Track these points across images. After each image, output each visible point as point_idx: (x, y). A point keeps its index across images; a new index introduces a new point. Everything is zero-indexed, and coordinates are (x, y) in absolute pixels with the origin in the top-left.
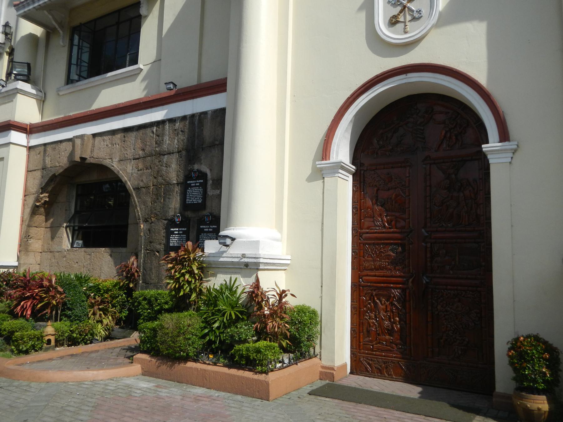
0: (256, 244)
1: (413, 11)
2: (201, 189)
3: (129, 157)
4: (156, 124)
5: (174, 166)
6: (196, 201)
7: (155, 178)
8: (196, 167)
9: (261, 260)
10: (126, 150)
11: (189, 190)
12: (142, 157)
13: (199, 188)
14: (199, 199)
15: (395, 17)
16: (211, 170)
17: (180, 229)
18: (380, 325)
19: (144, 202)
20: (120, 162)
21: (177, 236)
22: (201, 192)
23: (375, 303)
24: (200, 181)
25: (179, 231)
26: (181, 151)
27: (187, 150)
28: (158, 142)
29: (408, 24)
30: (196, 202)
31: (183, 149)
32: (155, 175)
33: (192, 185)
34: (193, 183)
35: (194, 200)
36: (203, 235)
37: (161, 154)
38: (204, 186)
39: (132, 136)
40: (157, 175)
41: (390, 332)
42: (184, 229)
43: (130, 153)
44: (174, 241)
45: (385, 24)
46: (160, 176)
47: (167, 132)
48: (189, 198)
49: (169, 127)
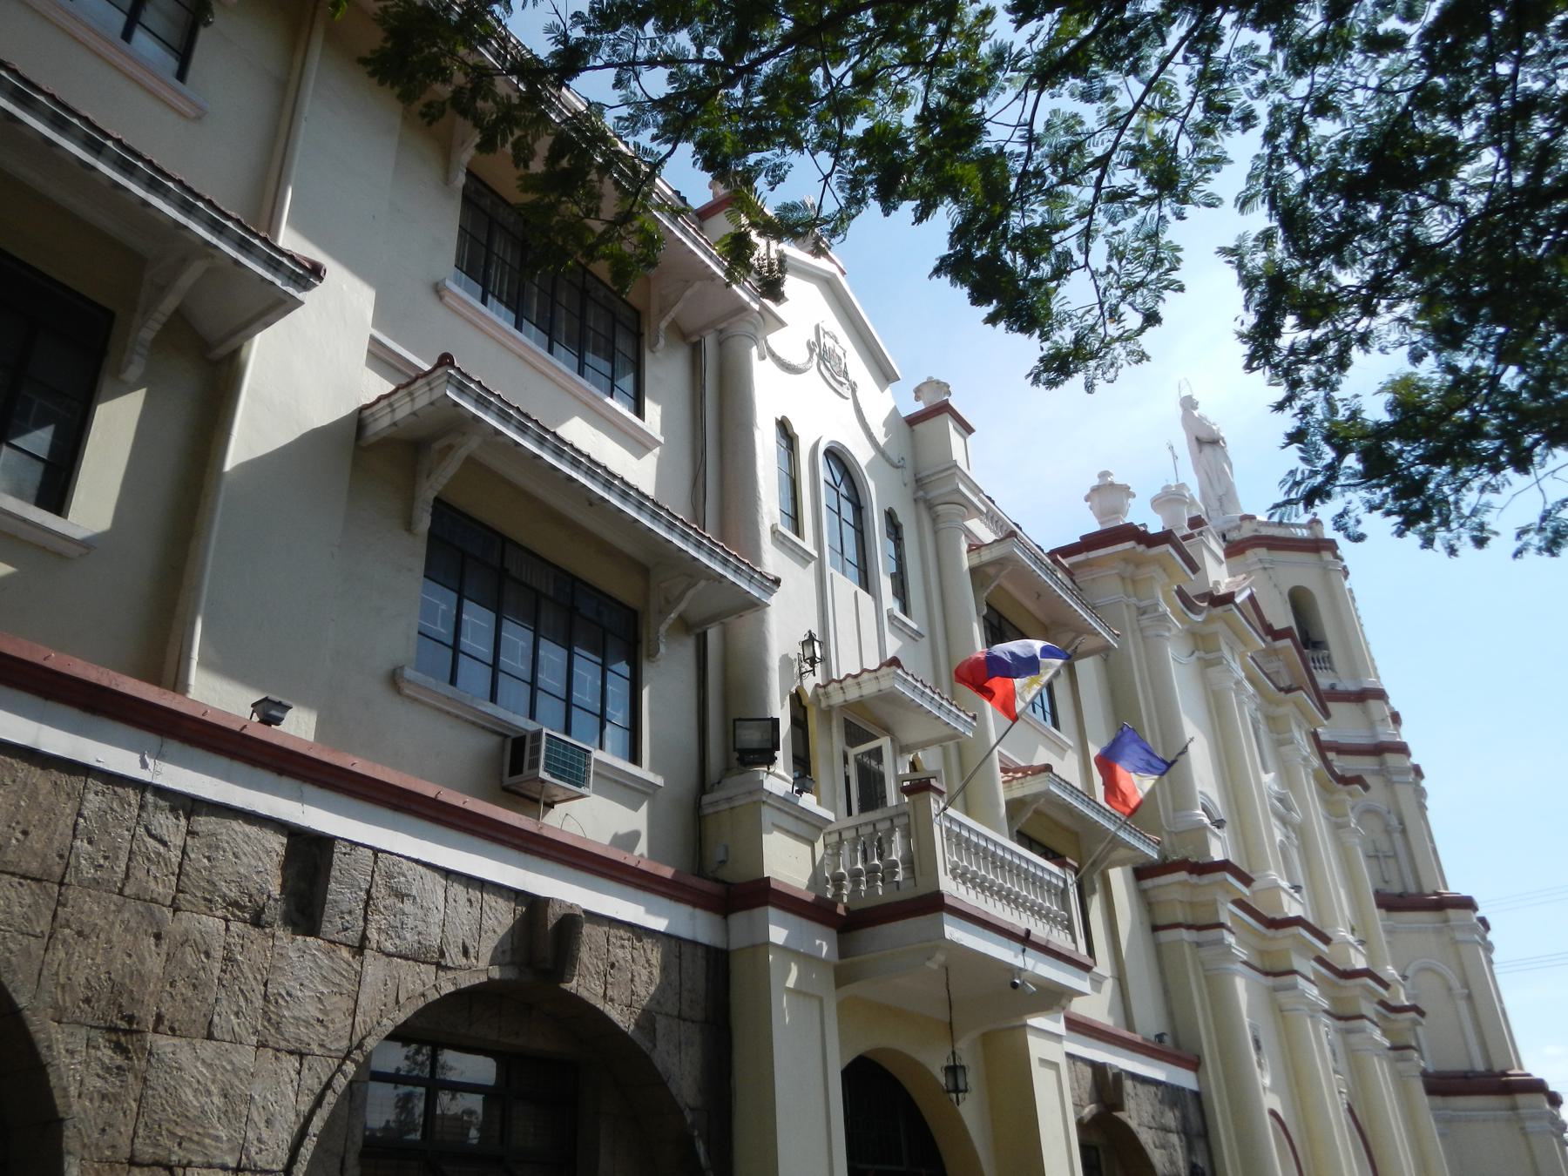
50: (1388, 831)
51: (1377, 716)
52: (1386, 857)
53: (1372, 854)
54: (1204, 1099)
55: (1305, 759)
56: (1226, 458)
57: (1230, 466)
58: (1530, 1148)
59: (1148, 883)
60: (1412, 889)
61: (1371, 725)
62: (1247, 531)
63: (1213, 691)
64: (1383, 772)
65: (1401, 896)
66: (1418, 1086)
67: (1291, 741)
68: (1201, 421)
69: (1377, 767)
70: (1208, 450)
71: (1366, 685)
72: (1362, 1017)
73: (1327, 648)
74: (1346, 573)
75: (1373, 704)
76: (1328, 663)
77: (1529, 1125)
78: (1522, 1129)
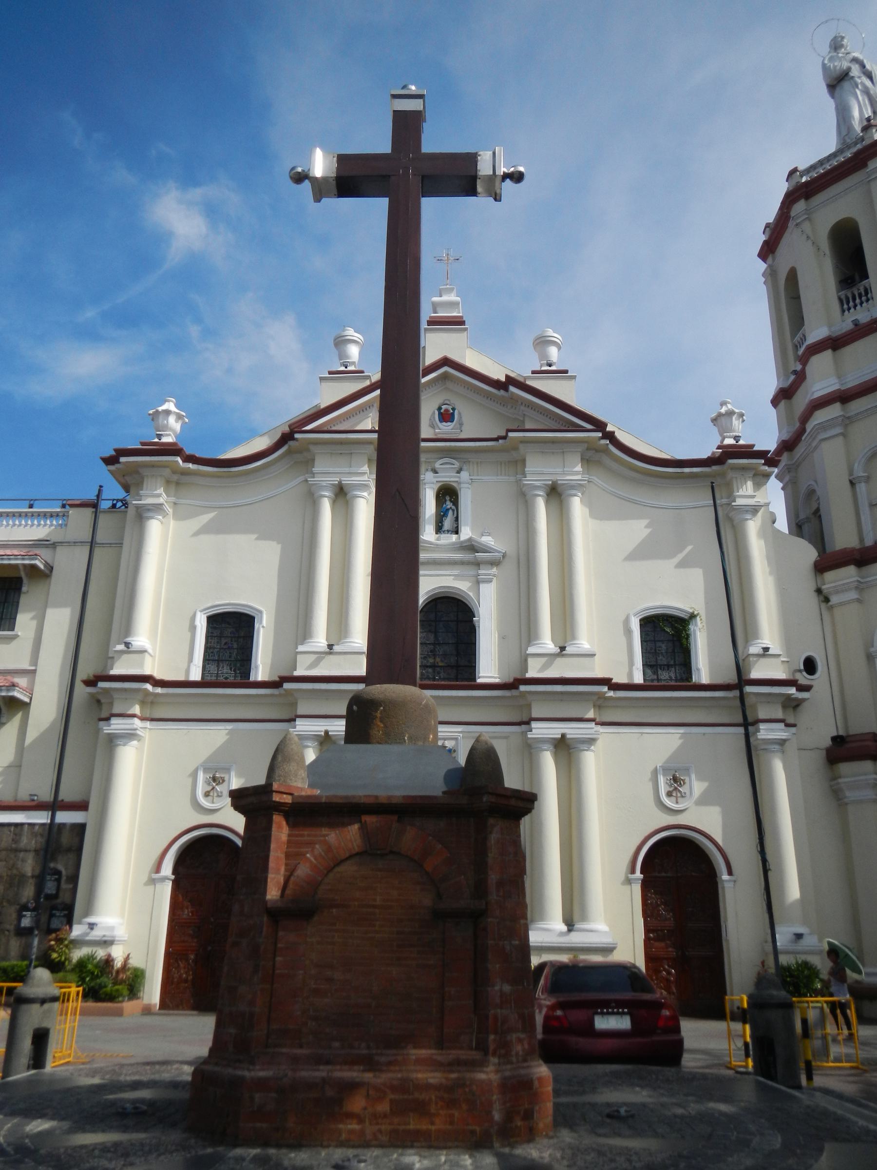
0: (112, 928)
1: (218, 791)
2: (55, 883)
8: (52, 865)
9: (117, 939)
15: (209, 792)
16: (66, 869)
18: (180, 976)
23: (178, 964)
26: (37, 851)
27: (46, 850)
29: (215, 798)
37: (17, 851)
38: (58, 881)
41: (186, 981)
45: (202, 794)
47: (26, 834)
49: (28, 829)
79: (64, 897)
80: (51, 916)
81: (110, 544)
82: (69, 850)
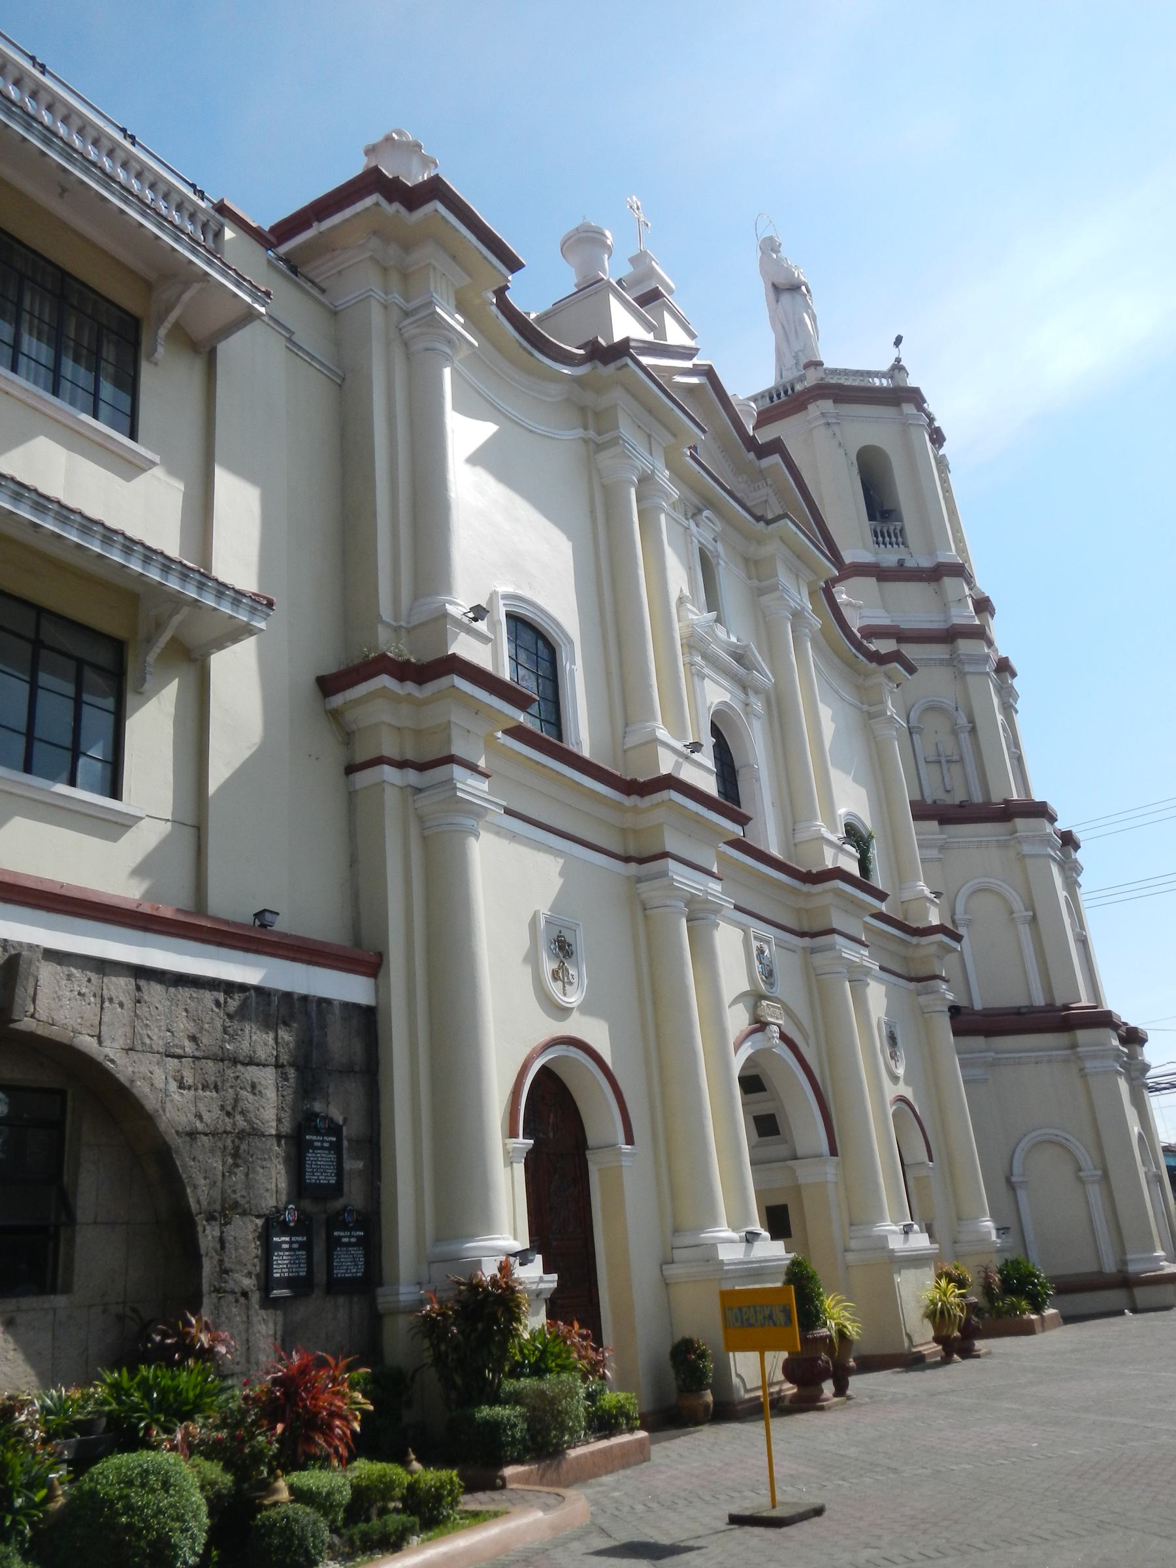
2: (333, 1156)
3: (155, 1048)
4: (223, 986)
5: (271, 1094)
6: (325, 1179)
7: (228, 1114)
8: (318, 1107)
10: (147, 1025)
11: (310, 1155)
12: (191, 1055)
13: (330, 1154)
14: (331, 1176)
17: (293, 1239)
19: (206, 1171)
20: (130, 1052)
21: (287, 1253)
22: (332, 1162)
24: (330, 1138)
25: (291, 1243)
26: (283, 1066)
28: (232, 1032)
30: (325, 1182)
31: (288, 1063)
32: (229, 1108)
33: (316, 1144)
34: (318, 1141)
35: (320, 1177)
36: (340, 1251)
38: (337, 1148)
39: (155, 992)
40: (233, 1108)
42: (300, 1239)
43: (158, 1038)
44: (281, 1266)
46: (240, 1113)
48: (310, 1172)
50: (955, 732)
51: (951, 596)
52: (948, 762)
53: (933, 759)
54: (381, 1018)
55: (797, 615)
56: (808, 307)
57: (814, 318)
58: (1088, 1092)
59: (338, 700)
60: (978, 798)
61: (945, 606)
62: (812, 378)
63: (604, 487)
64: (954, 663)
65: (962, 805)
66: (944, 1023)
67: (775, 588)
68: (779, 262)
69: (948, 657)
70: (786, 298)
71: (942, 560)
72: (832, 931)
73: (900, 519)
74: (938, 438)
75: (948, 582)
76: (898, 537)
77: (1089, 1064)
78: (1082, 1070)
79: (354, 1195)
80: (333, 1244)
81: (313, 358)
82: (348, 1071)
